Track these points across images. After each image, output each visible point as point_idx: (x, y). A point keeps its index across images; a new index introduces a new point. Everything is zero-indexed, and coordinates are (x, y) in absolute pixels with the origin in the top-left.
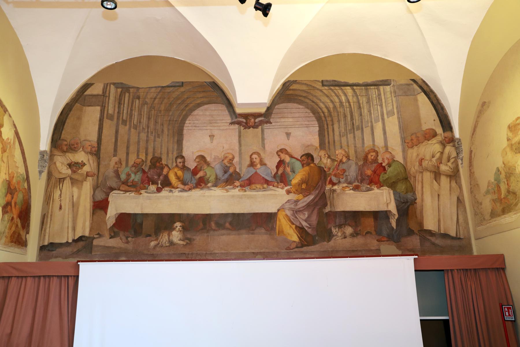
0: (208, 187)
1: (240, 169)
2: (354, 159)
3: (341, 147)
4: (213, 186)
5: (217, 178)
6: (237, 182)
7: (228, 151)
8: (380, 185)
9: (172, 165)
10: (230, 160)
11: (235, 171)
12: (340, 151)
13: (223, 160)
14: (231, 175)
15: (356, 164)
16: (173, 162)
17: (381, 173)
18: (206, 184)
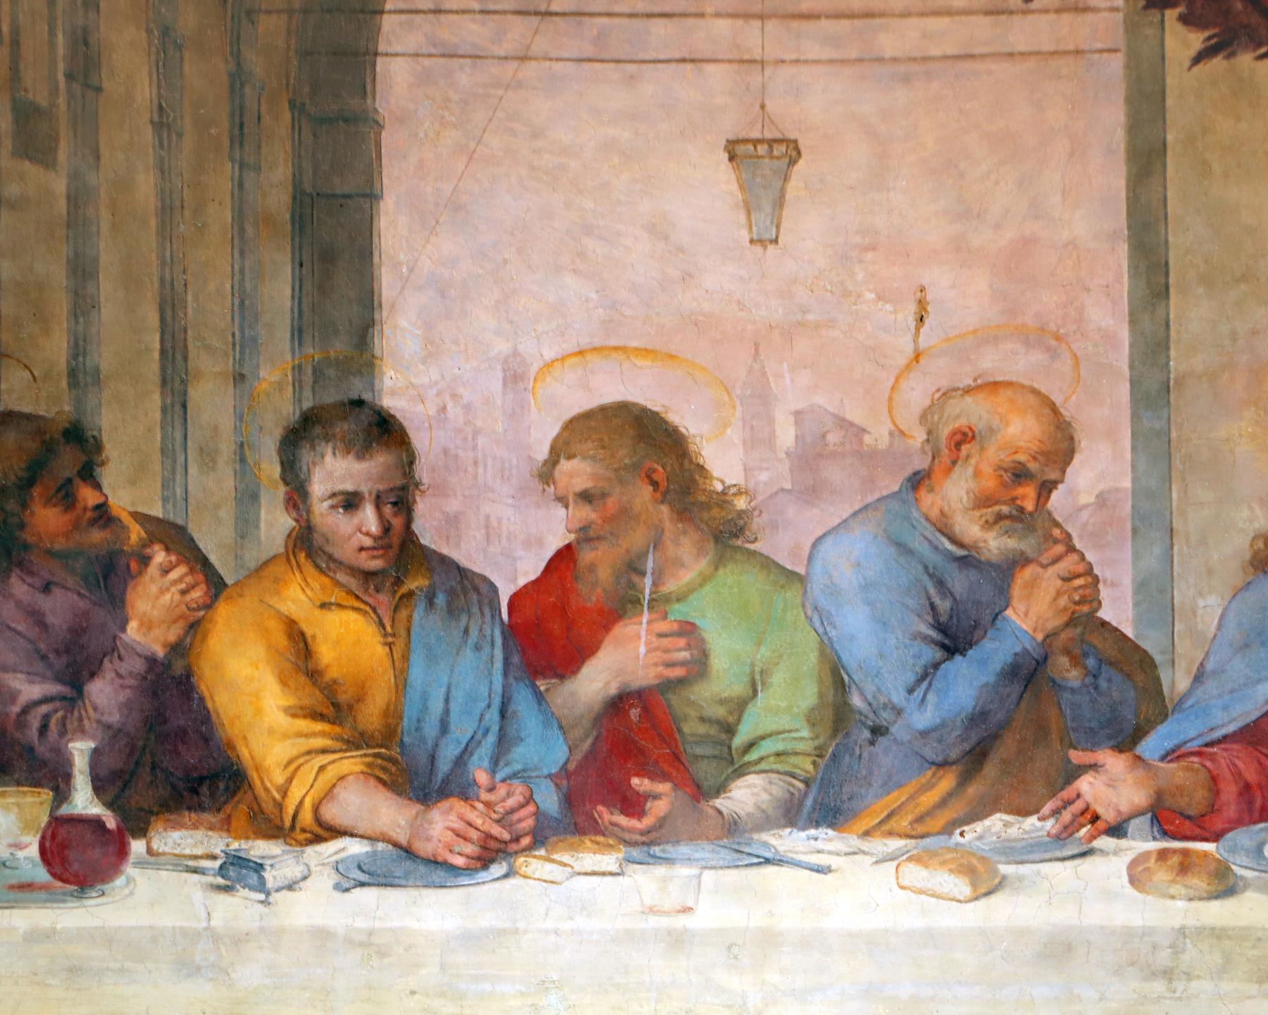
0: (731, 830)
1: (1156, 594)
4: (791, 814)
5: (844, 718)
6: (1115, 763)
7: (990, 362)
9: (246, 525)
10: (1020, 474)
11: (1084, 621)
13: (917, 481)
14: (1028, 674)
16: (248, 497)
18: (700, 792)
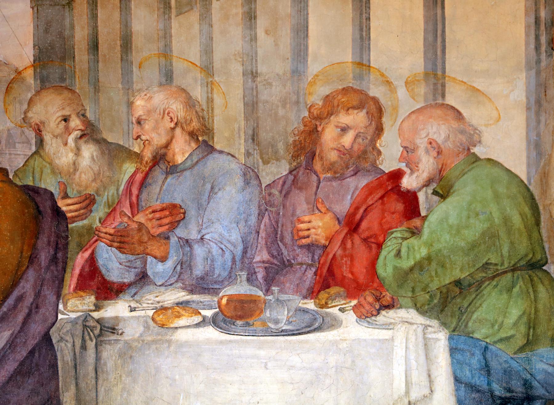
2: (240, 148)
3: (168, 77)
8: (374, 296)
12: (159, 98)
15: (250, 175)
17: (386, 232)
